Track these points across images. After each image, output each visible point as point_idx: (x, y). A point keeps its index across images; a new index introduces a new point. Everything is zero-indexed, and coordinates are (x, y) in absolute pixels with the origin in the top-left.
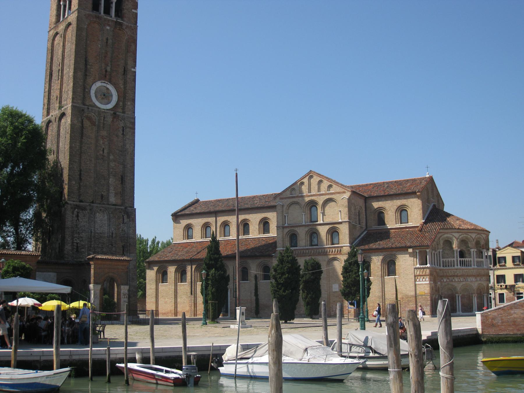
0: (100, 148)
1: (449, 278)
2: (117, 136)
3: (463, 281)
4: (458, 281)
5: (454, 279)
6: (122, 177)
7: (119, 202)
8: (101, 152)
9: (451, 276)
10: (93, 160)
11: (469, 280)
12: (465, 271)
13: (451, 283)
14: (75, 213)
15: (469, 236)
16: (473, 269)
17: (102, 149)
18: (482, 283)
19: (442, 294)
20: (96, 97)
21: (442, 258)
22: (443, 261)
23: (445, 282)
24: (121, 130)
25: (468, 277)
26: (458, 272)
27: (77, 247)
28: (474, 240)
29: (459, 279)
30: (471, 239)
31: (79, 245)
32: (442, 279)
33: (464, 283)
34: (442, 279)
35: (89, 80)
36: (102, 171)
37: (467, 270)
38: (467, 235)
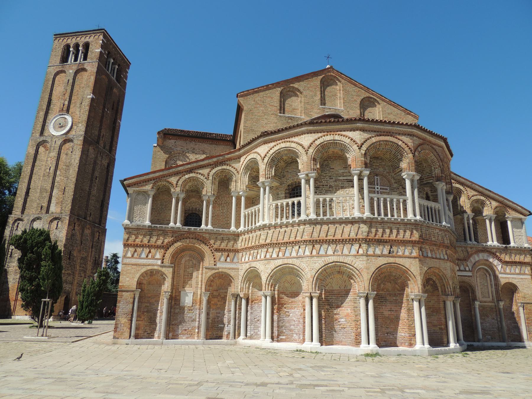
0: (47, 167)
2: (67, 154)
4: (266, 259)
6: (65, 188)
7: (58, 210)
8: (48, 170)
10: (42, 178)
11: (294, 254)
14: (16, 224)
15: (293, 145)
16: (305, 223)
17: (49, 168)
18: (348, 260)
20: (54, 128)
24: (71, 149)
27: (11, 253)
28: (307, 151)
30: (300, 148)
31: (13, 251)
33: (279, 262)
35: (50, 117)
36: (45, 186)
38: (288, 145)
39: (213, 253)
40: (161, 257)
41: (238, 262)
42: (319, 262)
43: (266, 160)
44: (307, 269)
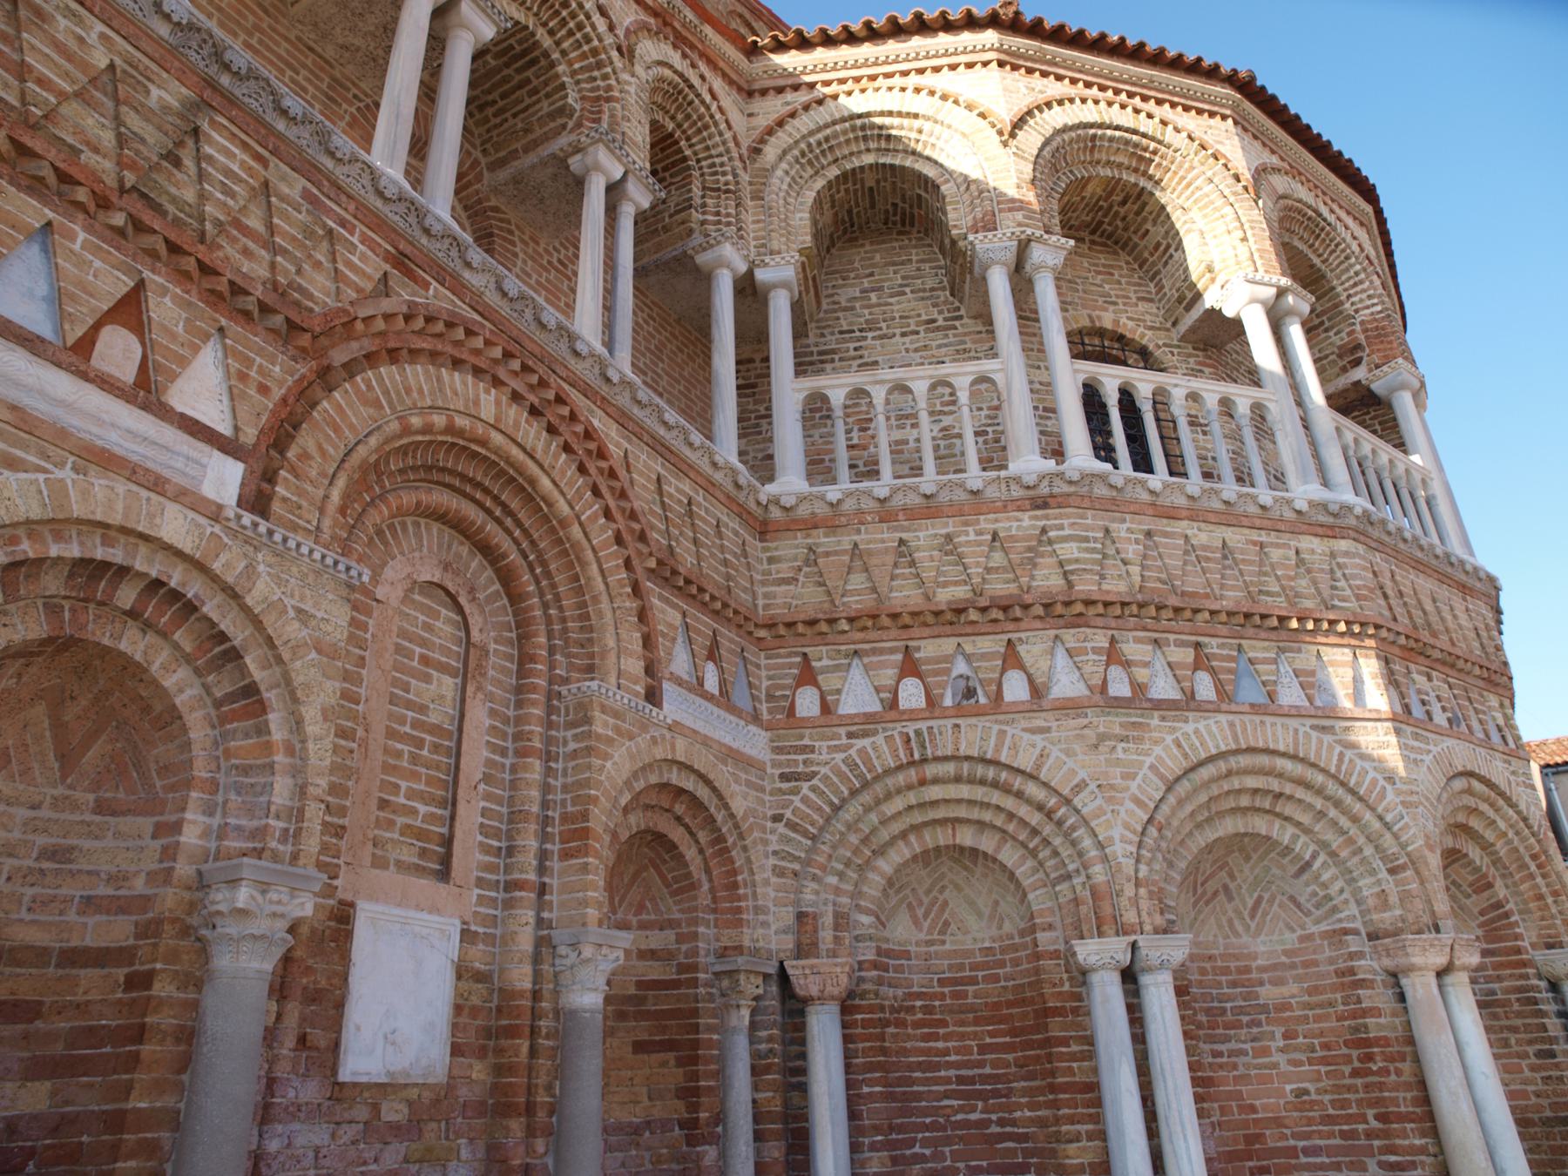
1: (928, 649)
3: (1188, 703)
5: (1011, 658)
9: (952, 618)
12: (1203, 536)
13: (974, 736)
19: (801, 952)
21: (803, 366)
22: (816, 410)
23: (866, 724)
25: (1258, 649)
26: (1069, 550)
29: (1113, 655)
32: (807, 676)
34: (807, 676)
37: (1235, 537)
39: (637, 590)
40: (250, 435)
41: (756, 718)
42: (1428, 759)
43: (1031, 139)
44: (1390, 796)
